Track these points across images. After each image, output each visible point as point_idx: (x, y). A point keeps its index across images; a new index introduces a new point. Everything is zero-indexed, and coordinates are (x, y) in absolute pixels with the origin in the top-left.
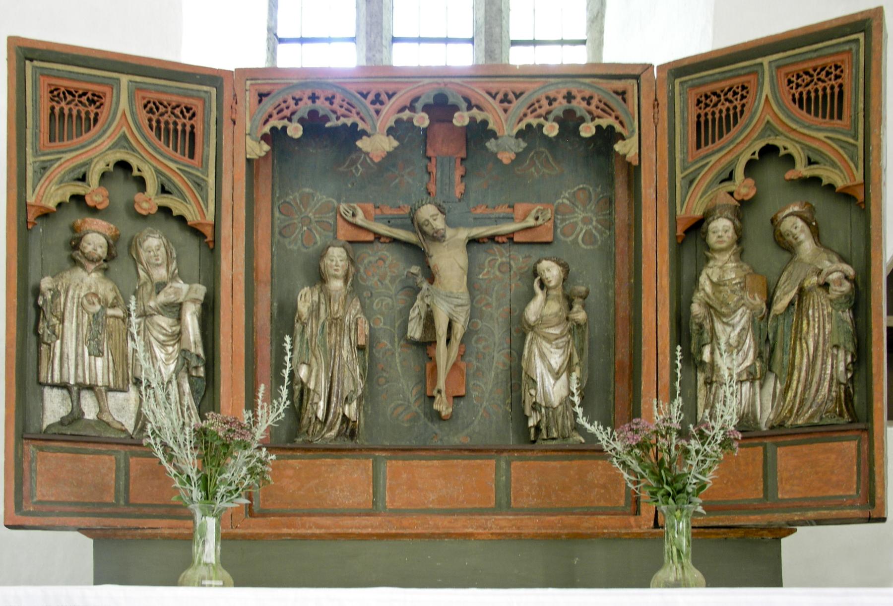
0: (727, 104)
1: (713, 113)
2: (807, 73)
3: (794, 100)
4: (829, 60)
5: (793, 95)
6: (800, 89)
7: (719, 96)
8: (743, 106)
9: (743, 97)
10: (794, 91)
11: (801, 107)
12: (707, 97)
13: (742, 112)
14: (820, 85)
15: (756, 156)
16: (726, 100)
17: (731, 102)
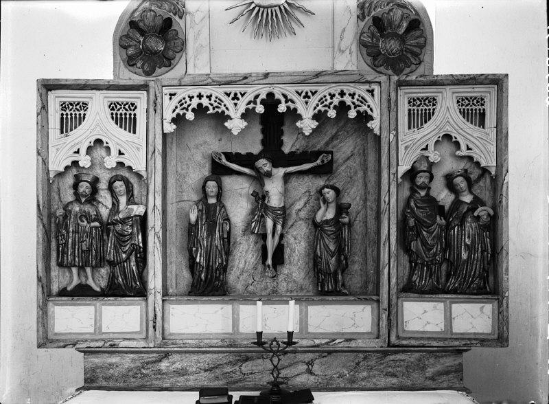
0: (425, 107)
1: (418, 110)
2: (467, 99)
3: (460, 112)
4: (479, 94)
5: (460, 109)
6: (464, 107)
7: (421, 101)
8: (434, 109)
9: (434, 105)
10: (460, 107)
11: (464, 117)
12: (414, 100)
13: (433, 113)
14: (474, 107)
15: (440, 139)
16: (425, 104)
17: (427, 106)
